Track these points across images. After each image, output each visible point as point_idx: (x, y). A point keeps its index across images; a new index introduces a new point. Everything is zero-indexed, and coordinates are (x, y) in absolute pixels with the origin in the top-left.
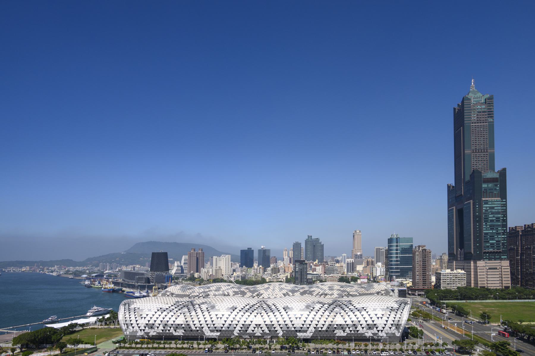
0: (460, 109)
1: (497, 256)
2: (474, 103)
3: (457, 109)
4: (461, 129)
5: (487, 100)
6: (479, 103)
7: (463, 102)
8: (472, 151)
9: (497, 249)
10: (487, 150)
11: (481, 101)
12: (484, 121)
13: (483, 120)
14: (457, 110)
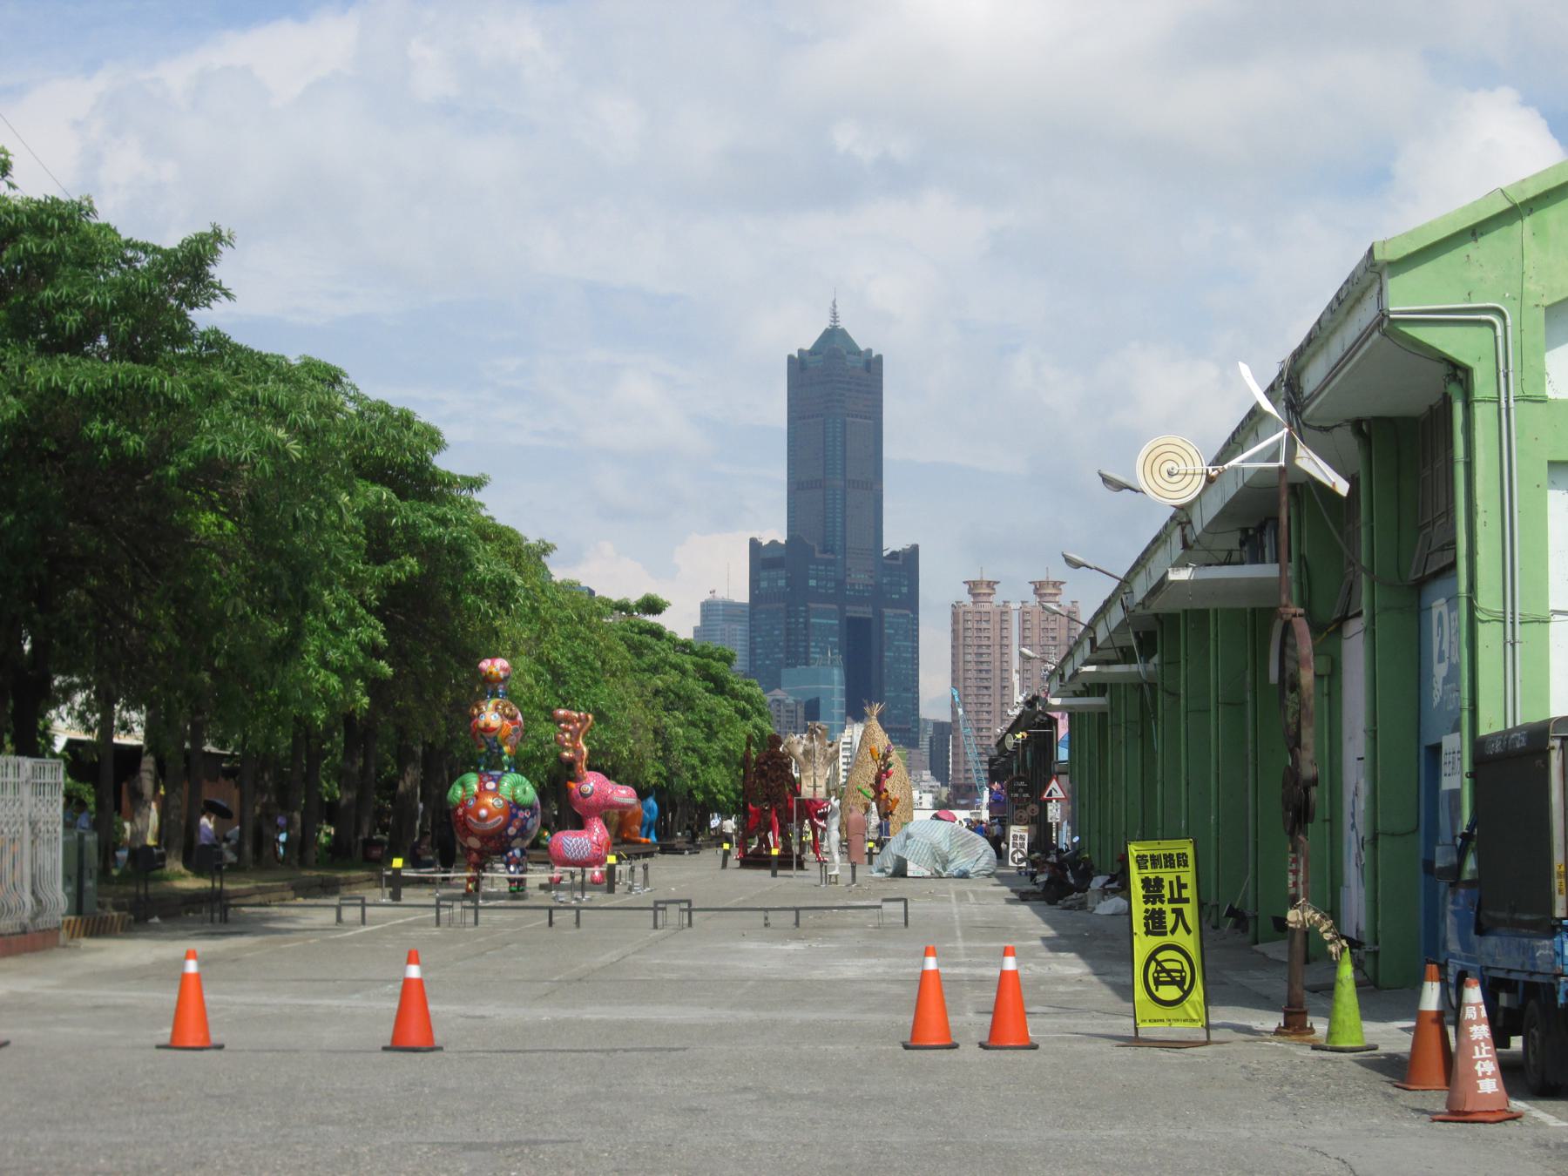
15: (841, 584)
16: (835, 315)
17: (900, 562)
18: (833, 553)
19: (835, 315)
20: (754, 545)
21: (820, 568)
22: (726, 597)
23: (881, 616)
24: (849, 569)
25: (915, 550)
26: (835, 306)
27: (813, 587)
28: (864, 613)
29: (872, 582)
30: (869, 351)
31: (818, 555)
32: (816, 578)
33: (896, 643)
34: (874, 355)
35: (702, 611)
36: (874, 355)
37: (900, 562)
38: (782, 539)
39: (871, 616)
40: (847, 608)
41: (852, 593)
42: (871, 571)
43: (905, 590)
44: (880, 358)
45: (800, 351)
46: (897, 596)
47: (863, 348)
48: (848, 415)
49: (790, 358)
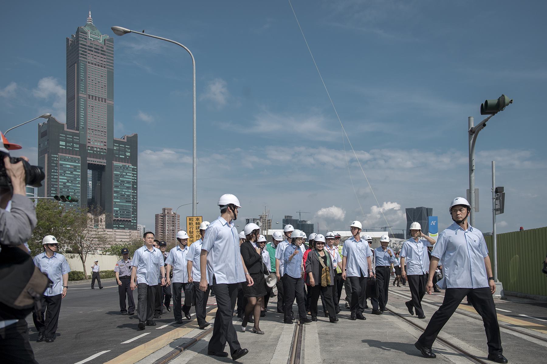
0: (74, 42)
1: (120, 225)
2: (91, 40)
3: (71, 41)
4: (75, 66)
5: (106, 42)
6: (97, 41)
7: (77, 32)
8: (88, 96)
9: (121, 217)
10: (105, 99)
11: (100, 40)
12: (102, 65)
13: (101, 64)
14: (70, 42)
15: (83, 147)
17: (125, 140)
18: (78, 130)
21: (67, 136)
23: (112, 164)
24: (89, 140)
25: (136, 136)
27: (62, 145)
28: (102, 162)
29: (105, 147)
31: (66, 129)
32: (66, 141)
33: (120, 179)
37: (125, 140)
39: (105, 164)
40: (88, 159)
41: (92, 152)
42: (105, 142)
43: (128, 154)
46: (124, 157)
48: (89, 63)
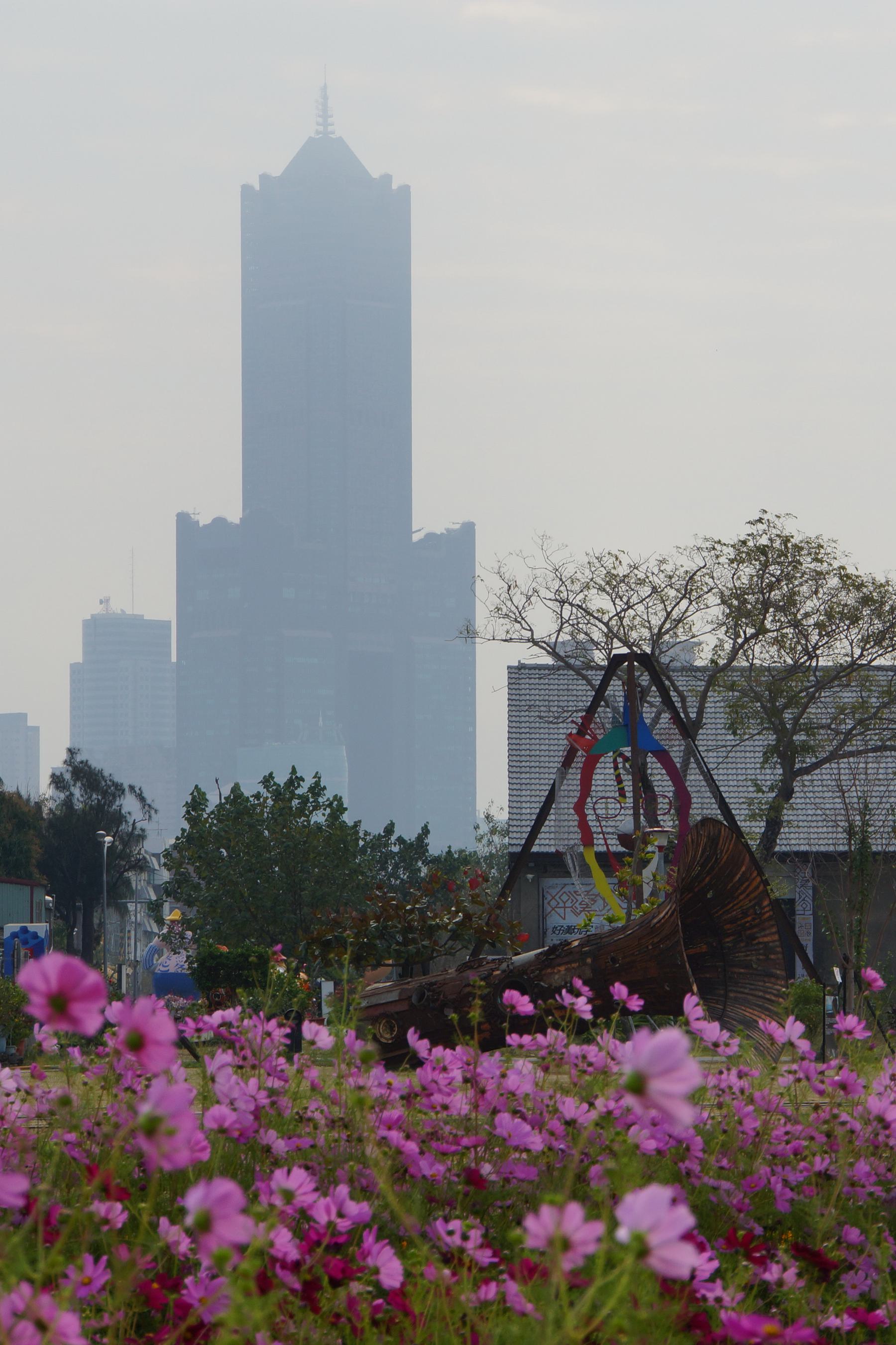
16: (325, 114)
19: (325, 114)
20: (184, 522)
22: (129, 611)
25: (469, 529)
26: (325, 98)
30: (387, 178)
34: (395, 186)
35: (85, 635)
36: (395, 186)
38: (234, 515)
44: (405, 190)
45: (264, 178)
47: (375, 173)
49: (246, 190)
